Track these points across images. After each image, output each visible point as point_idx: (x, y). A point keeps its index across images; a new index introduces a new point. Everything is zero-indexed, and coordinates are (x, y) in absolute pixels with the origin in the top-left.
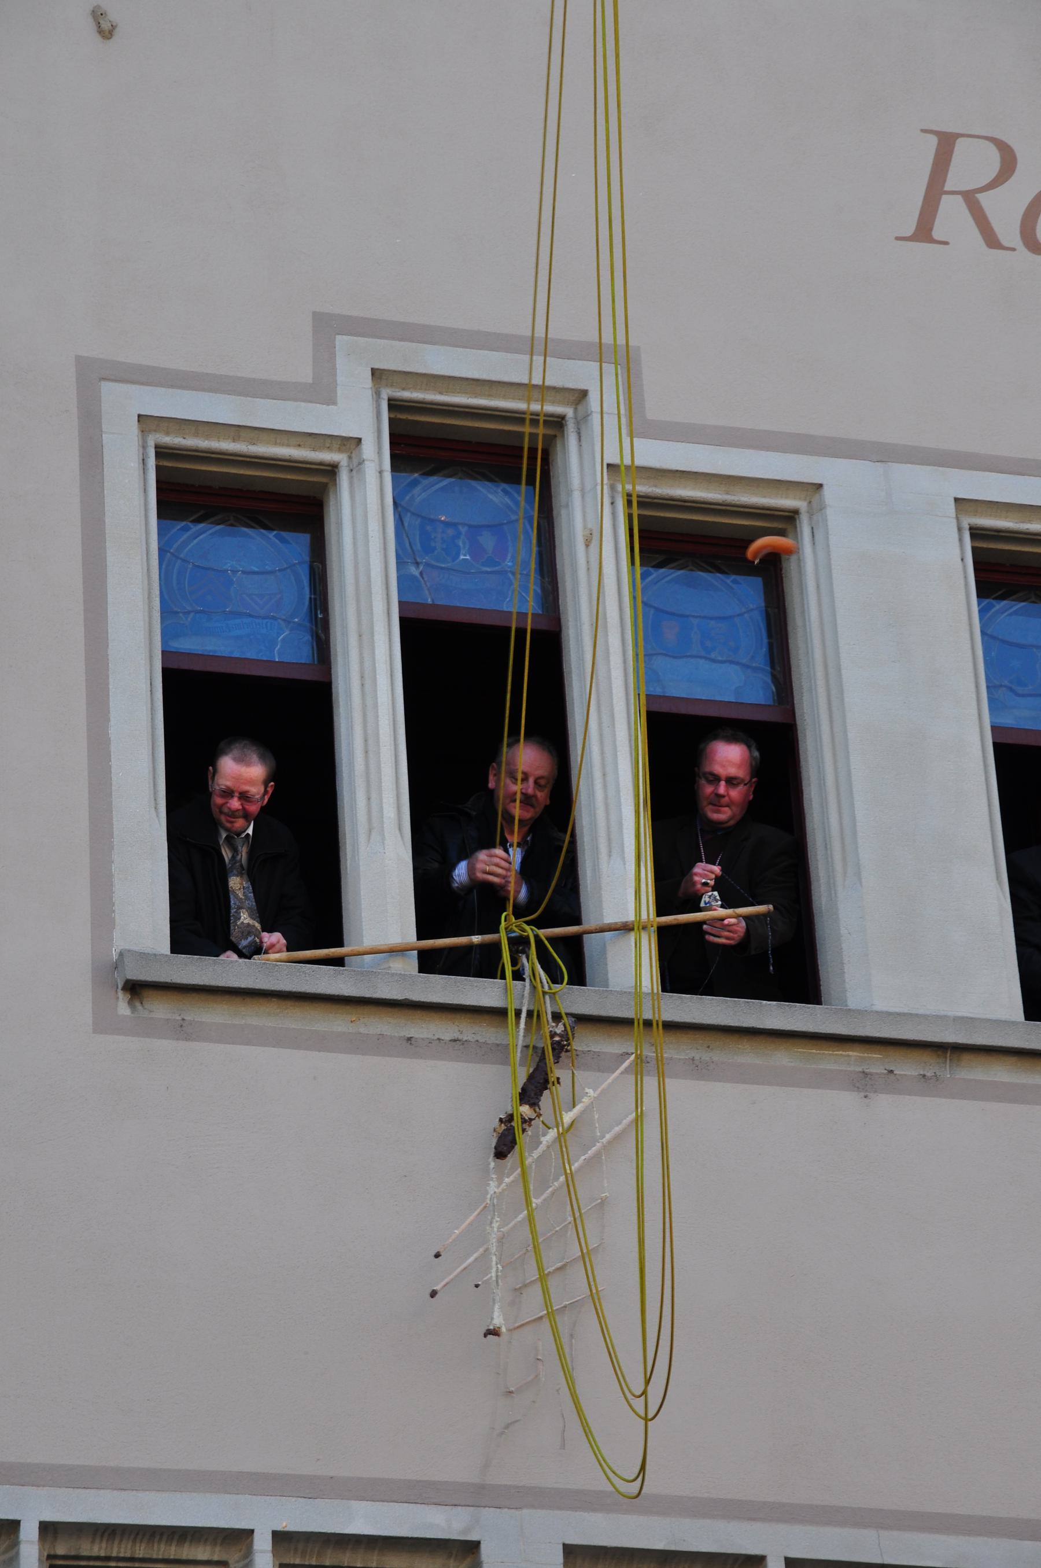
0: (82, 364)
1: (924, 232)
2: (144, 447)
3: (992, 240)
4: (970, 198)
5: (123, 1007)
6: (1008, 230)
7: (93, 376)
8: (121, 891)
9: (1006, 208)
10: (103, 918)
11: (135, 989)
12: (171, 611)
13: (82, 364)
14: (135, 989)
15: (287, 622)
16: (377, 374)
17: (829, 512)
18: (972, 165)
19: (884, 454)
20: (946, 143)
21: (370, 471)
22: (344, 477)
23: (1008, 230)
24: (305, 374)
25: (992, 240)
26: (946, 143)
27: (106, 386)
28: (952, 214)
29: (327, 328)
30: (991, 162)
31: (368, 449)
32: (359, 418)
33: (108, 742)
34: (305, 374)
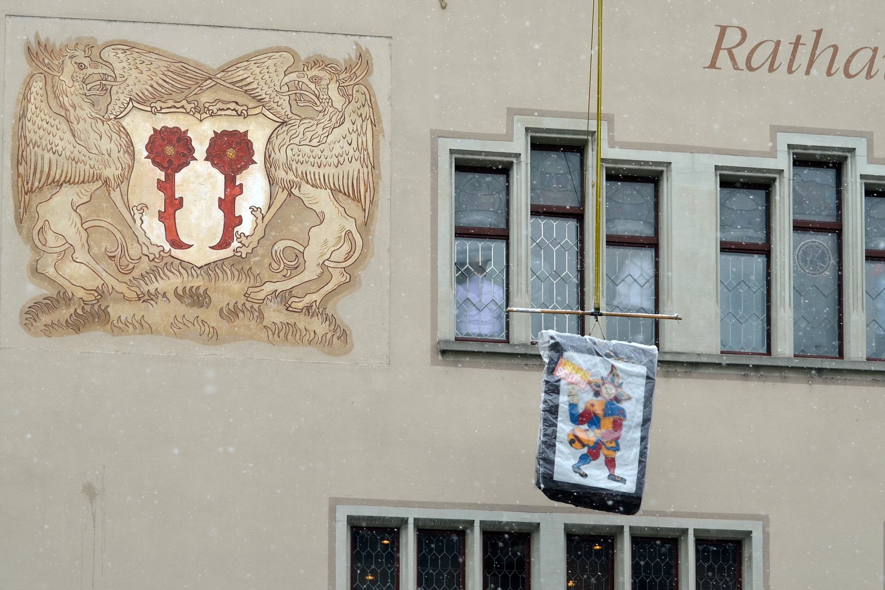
0: (432, 132)
1: (713, 65)
2: (451, 158)
3: (736, 67)
4: (730, 51)
5: (440, 357)
6: (742, 63)
7: (438, 135)
8: (440, 318)
9: (740, 55)
10: (434, 327)
11: (444, 352)
12: (458, 210)
13: (432, 132)
14: (444, 352)
15: (496, 212)
16: (527, 129)
17: (673, 172)
20: (723, 29)
21: (523, 165)
22: (515, 166)
23: (742, 63)
24: (504, 131)
26: (723, 29)
27: (440, 140)
28: (723, 58)
29: (512, 113)
30: (738, 37)
31: (523, 157)
32: (520, 145)
33: (437, 267)
34: (504, 131)
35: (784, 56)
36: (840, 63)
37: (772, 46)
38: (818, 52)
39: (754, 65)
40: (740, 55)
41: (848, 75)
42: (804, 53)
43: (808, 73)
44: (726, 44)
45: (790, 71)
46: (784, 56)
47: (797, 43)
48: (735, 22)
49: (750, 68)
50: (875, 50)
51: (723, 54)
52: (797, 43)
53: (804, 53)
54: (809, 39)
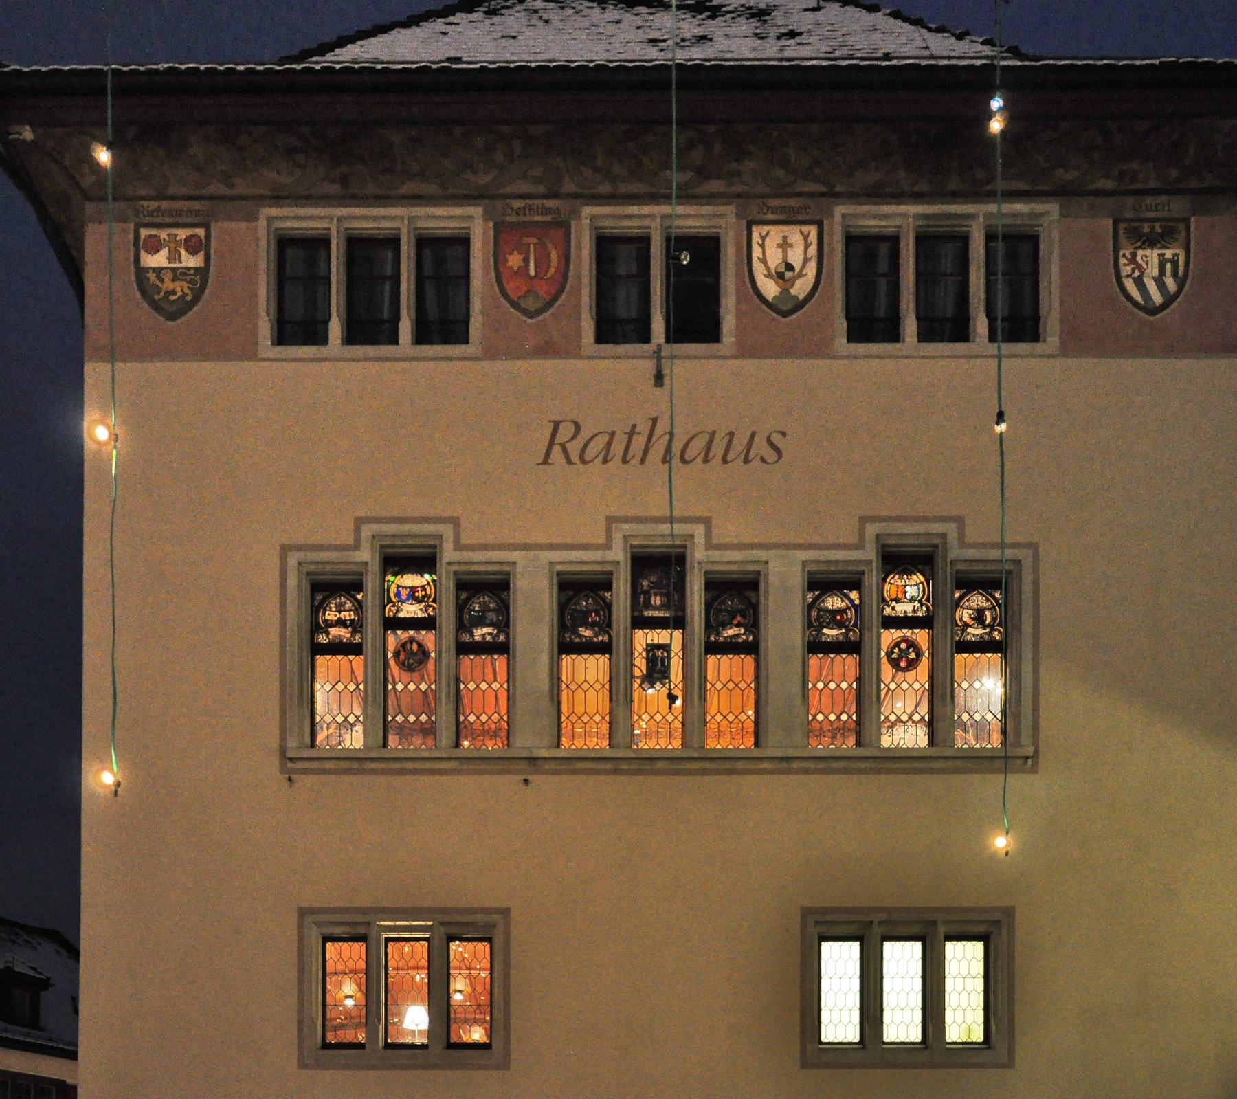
3: (569, 461)
6: (575, 458)
9: (574, 448)
18: (565, 433)
19: (526, 547)
20: (557, 424)
23: (575, 458)
25: (569, 461)
26: (557, 424)
35: (618, 448)
36: (677, 447)
37: (606, 438)
38: (654, 439)
39: (587, 458)
40: (574, 448)
41: (683, 460)
42: (639, 442)
43: (643, 461)
44: (559, 439)
45: (625, 461)
46: (618, 448)
47: (632, 433)
48: (572, 415)
49: (583, 461)
50: (713, 434)
51: (557, 449)
52: (632, 433)
53: (639, 442)
54: (644, 428)
